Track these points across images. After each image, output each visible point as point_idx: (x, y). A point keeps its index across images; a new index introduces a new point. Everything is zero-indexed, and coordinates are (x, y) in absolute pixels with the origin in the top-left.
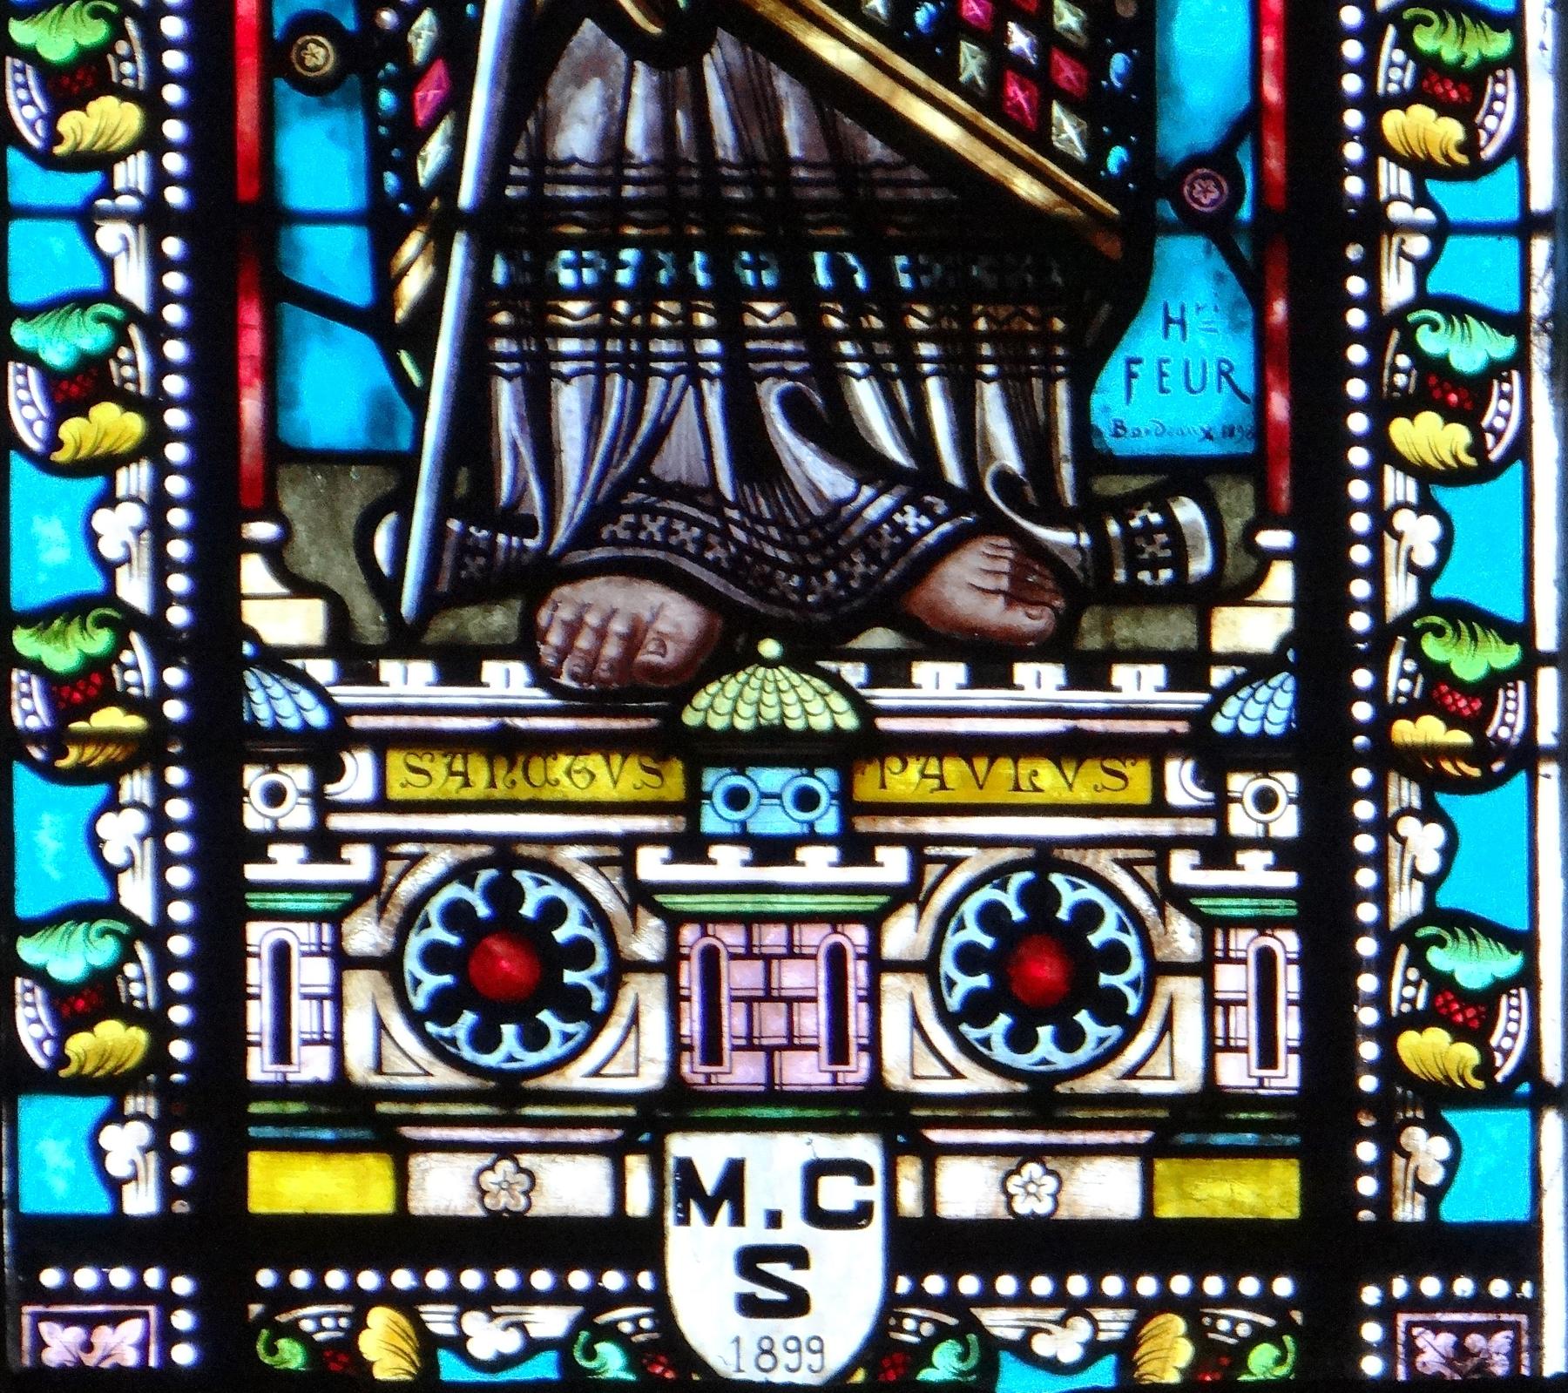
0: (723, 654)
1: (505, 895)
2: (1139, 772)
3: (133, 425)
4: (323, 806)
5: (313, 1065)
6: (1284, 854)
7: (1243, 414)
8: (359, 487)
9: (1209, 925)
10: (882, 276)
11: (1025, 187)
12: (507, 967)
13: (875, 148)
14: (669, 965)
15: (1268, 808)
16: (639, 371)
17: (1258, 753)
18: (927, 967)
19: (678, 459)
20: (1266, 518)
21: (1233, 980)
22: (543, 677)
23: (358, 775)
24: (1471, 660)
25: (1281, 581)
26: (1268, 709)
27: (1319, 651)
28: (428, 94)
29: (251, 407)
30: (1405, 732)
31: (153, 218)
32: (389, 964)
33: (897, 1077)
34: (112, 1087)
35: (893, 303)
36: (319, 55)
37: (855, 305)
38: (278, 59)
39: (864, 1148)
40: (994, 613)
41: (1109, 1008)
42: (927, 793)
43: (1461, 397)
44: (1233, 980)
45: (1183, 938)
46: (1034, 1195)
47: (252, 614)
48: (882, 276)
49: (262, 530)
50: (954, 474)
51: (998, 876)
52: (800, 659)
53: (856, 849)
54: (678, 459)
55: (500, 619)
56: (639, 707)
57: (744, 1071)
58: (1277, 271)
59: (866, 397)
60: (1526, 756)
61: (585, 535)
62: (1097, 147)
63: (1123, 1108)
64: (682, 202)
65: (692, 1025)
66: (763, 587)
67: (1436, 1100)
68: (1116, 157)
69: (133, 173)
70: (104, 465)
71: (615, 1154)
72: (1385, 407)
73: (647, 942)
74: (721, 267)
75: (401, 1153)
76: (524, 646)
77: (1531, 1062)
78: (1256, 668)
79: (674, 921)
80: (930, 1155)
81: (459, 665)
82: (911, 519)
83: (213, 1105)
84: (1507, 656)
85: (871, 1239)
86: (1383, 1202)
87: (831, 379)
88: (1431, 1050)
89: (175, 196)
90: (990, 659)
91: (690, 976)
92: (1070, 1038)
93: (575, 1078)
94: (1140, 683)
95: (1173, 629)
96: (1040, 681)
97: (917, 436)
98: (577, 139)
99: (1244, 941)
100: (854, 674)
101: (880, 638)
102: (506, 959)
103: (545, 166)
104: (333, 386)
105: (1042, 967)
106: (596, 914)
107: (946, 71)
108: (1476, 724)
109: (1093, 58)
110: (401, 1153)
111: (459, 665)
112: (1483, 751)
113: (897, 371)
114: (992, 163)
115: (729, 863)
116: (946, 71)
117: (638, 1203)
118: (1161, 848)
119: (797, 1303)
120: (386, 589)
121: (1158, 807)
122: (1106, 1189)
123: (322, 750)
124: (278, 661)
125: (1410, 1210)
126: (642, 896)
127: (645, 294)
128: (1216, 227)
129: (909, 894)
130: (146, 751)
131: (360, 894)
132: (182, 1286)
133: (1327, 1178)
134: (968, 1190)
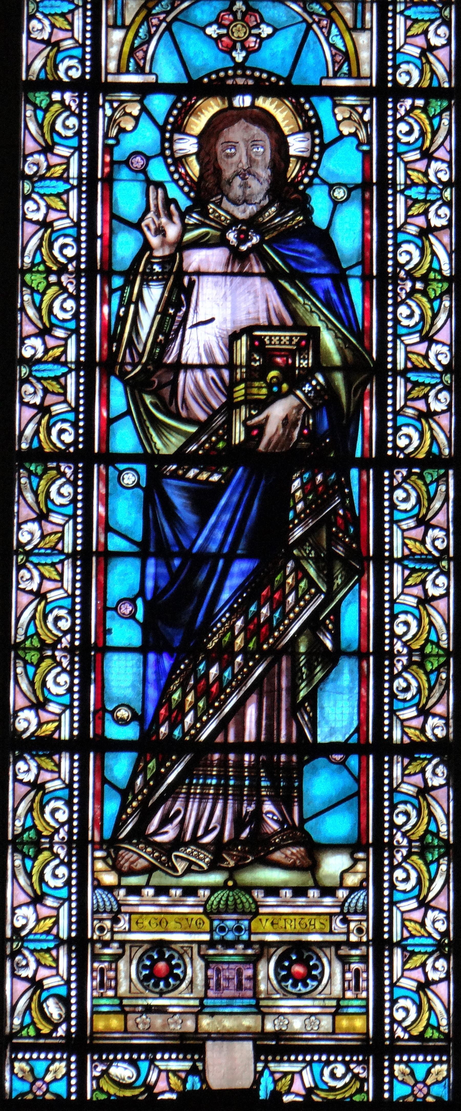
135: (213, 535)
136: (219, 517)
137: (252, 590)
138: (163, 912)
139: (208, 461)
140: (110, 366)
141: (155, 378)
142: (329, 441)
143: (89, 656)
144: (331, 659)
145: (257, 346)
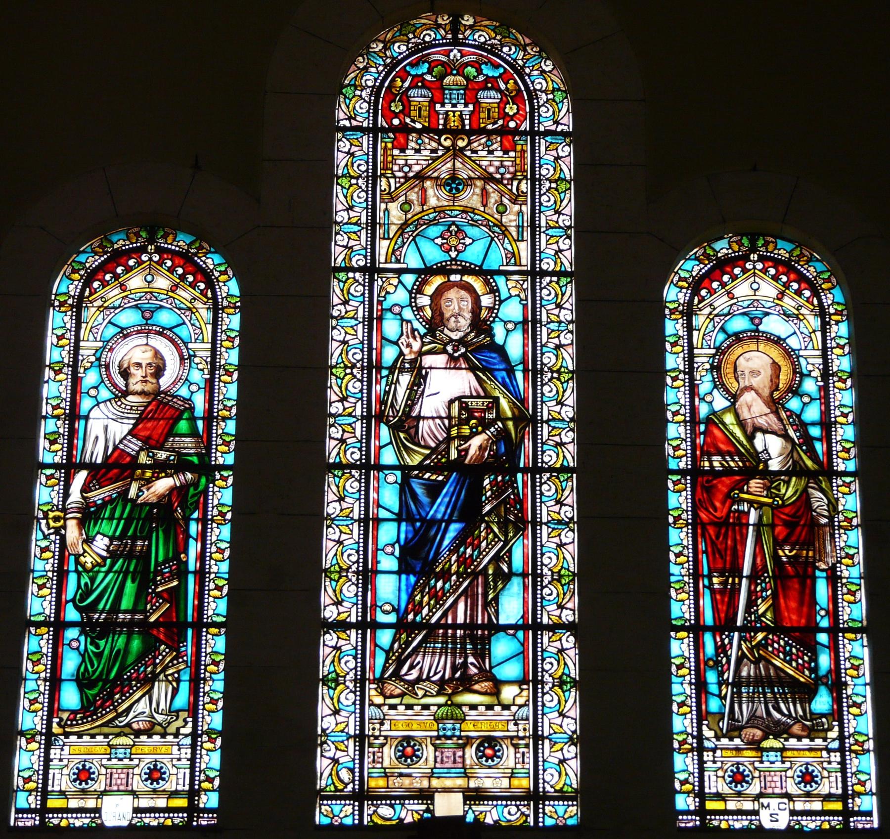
0: (765, 737)
1: (738, 768)
2: (819, 753)
3: (689, 709)
4: (714, 757)
5: (714, 790)
6: (839, 763)
7: (830, 708)
8: (717, 717)
9: (829, 772)
10: (784, 690)
11: (802, 679)
12: (738, 778)
13: (782, 675)
14: (760, 777)
15: (836, 757)
16: (753, 702)
17: (834, 750)
18: (793, 777)
19: (758, 713)
20: (834, 721)
21: (832, 779)
22: (742, 741)
23: (718, 753)
24: (861, 739)
25: (836, 729)
26: (835, 745)
27: (841, 738)
28: (725, 667)
29: (704, 707)
30: (853, 748)
31: (690, 684)
32: (723, 777)
33: (789, 792)
34: (688, 793)
35: (786, 694)
36: (711, 663)
37: (780, 694)
38: (706, 663)
39: (786, 800)
40: (800, 733)
41: (816, 783)
42: (792, 755)
43: (858, 705)
44: (832, 779)
45: (825, 774)
46: (808, 806)
47: (704, 733)
48: (784, 690)
49: (705, 722)
50: (794, 715)
51: (801, 766)
52: (775, 738)
53: (783, 762)
54: (758, 713)
55: (736, 733)
56: (755, 745)
57: (770, 791)
58: (834, 690)
59: (782, 706)
60: (868, 751)
61: (747, 723)
62: (811, 674)
63: (818, 796)
64: (758, 681)
65: (763, 785)
66: (770, 729)
67: (859, 794)
68: (813, 676)
69: (688, 678)
70: (685, 714)
71: (753, 801)
72: (849, 707)
73: (757, 774)
74: (763, 689)
75: (725, 801)
76: (739, 737)
77: (871, 790)
78: (834, 740)
79: (760, 771)
80: (794, 801)
81: (731, 739)
82: (789, 721)
83: (701, 795)
84: (866, 738)
85: (787, 812)
86: (853, 808)
87: (778, 703)
88: (858, 788)
89: (693, 681)
90: (799, 738)
91: (762, 778)
92: (811, 787)
93: (747, 792)
94: (819, 742)
95: (822, 735)
96: (806, 741)
97: (789, 710)
98: (744, 673)
99: (833, 774)
100: (782, 740)
101: (785, 736)
102: (739, 777)
103: (740, 677)
104: (714, 705)
105: (807, 777)
106: (750, 771)
107: (791, 665)
108: (862, 747)
109: (809, 664)
110: (725, 801)
111: (731, 739)
112: (863, 750)
113: (786, 702)
114: (797, 676)
115: (767, 764)
116: (791, 665)
117: (756, 808)
118: (822, 762)
119: (777, 821)
120: (722, 730)
121: (821, 757)
122: (817, 806)
123: (714, 750)
124: (708, 739)
125: (856, 809)
126: (755, 769)
127: (754, 693)
128: (826, 684)
129: (791, 768)
130: (691, 750)
131: (719, 768)
132: (698, 818)
133: (845, 805)
134: (799, 806)
135: (439, 509)
136: (443, 499)
137: (462, 539)
139: (436, 469)
140: (381, 417)
141: (406, 425)
142: (504, 459)
143: (368, 576)
144: (507, 578)
145: (464, 407)
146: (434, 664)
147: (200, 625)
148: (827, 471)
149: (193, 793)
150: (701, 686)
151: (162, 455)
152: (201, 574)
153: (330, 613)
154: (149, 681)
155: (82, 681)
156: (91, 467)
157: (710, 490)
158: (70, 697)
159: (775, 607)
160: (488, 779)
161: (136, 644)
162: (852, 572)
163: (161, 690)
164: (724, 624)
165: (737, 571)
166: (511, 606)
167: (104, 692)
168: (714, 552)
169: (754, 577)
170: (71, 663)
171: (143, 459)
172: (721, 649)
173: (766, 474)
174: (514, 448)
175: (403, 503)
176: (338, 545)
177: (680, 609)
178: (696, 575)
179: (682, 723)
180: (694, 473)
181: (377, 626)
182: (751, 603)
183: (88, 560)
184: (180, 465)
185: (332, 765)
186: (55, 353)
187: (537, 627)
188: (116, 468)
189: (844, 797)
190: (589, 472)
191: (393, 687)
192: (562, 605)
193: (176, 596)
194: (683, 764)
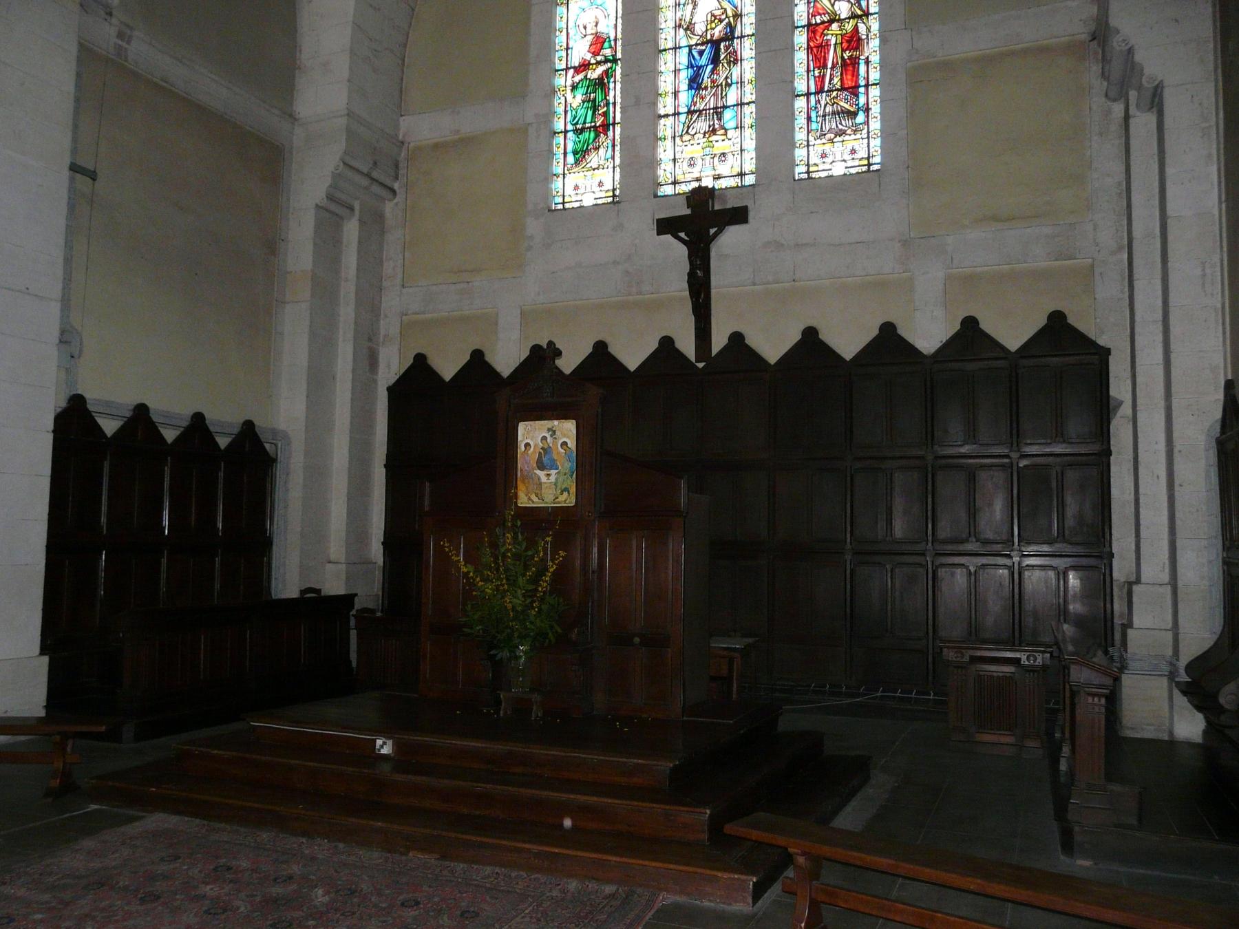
12: (824, 156)
56: (831, 141)
64: (833, 113)
83: (808, 165)
104: (814, 126)
135: (703, 61)
136: (705, 56)
137: (712, 72)
138: (693, 149)
139: (702, 44)
140: (680, 26)
141: (690, 28)
142: (729, 36)
143: (676, 94)
144: (730, 85)
145: (713, 15)
146: (702, 125)
147: (614, 124)
148: (867, 14)
149: (614, 190)
150: (809, 118)
151: (599, 58)
152: (614, 104)
153: (662, 112)
154: (597, 149)
155: (575, 153)
156: (574, 68)
157: (814, 32)
158: (571, 159)
159: (842, 79)
160: (723, 169)
161: (592, 135)
162: (875, 58)
163: (602, 151)
164: (820, 91)
165: (825, 66)
166: (732, 96)
167: (581, 154)
168: (816, 59)
169: (832, 68)
170: (570, 147)
171: (593, 61)
172: (818, 102)
173: (839, 20)
174: (731, 28)
175: (689, 61)
176: (665, 83)
177: (801, 85)
178: (808, 71)
179: (800, 136)
180: (809, 25)
181: (679, 114)
182: (831, 79)
183: (574, 106)
184: (606, 61)
185: (665, 172)
186: (560, 24)
187: (742, 104)
188: (584, 66)
189: (868, 158)
190: (760, 35)
191: (686, 137)
192: (749, 94)
193: (605, 114)
194: (800, 153)
